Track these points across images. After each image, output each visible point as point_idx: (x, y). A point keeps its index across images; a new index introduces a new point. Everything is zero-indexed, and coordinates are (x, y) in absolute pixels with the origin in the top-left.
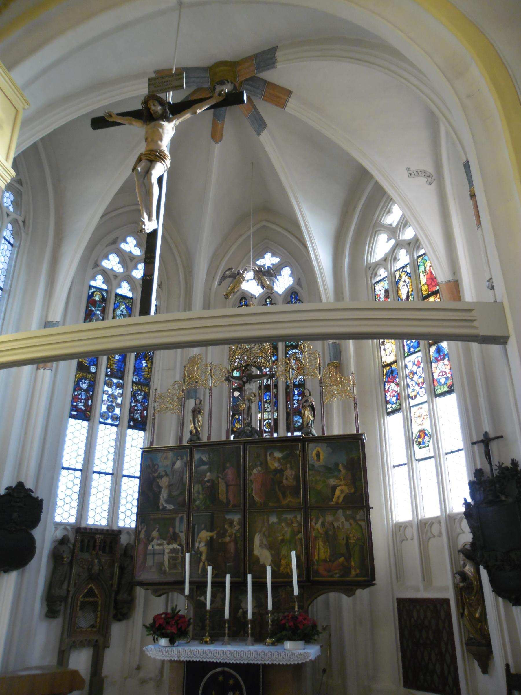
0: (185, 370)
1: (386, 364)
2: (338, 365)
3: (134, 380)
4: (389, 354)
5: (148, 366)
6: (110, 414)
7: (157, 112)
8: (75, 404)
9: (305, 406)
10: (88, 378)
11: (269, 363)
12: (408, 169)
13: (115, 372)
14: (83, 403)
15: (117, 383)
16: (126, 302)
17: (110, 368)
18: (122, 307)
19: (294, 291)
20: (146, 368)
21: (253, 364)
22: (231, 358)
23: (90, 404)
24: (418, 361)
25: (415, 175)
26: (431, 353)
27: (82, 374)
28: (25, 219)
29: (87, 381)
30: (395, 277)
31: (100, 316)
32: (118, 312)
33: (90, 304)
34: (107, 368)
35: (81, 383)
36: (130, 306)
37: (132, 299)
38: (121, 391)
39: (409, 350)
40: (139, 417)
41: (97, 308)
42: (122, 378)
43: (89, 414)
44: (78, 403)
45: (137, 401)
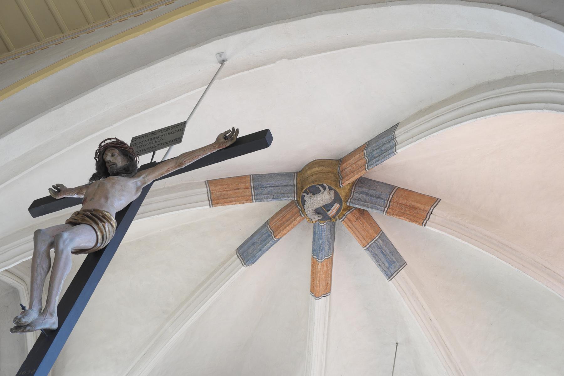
7: (115, 164)
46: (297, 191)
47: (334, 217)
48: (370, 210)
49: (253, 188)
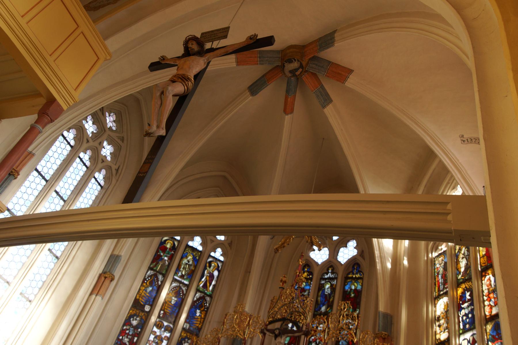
0: (225, 318)
1: (440, 342)
2: (386, 337)
3: (185, 326)
4: (443, 330)
5: (201, 316)
8: (121, 337)
10: (139, 316)
11: (306, 320)
12: (461, 136)
14: (129, 338)
15: (167, 326)
16: (194, 254)
17: (164, 310)
18: (190, 257)
19: (356, 262)
20: (200, 317)
21: (289, 318)
23: (135, 340)
24: (474, 339)
25: (468, 142)
26: (488, 331)
27: (136, 312)
28: (118, 168)
29: (138, 319)
30: (455, 249)
31: (167, 262)
32: (185, 261)
33: (161, 250)
34: (161, 310)
35: (132, 319)
36: (197, 258)
37: (200, 251)
38: (168, 335)
39: (464, 326)
41: (165, 254)
44: (124, 337)
46: (281, 61)
47: (299, 75)
48: (317, 73)
49: (259, 57)
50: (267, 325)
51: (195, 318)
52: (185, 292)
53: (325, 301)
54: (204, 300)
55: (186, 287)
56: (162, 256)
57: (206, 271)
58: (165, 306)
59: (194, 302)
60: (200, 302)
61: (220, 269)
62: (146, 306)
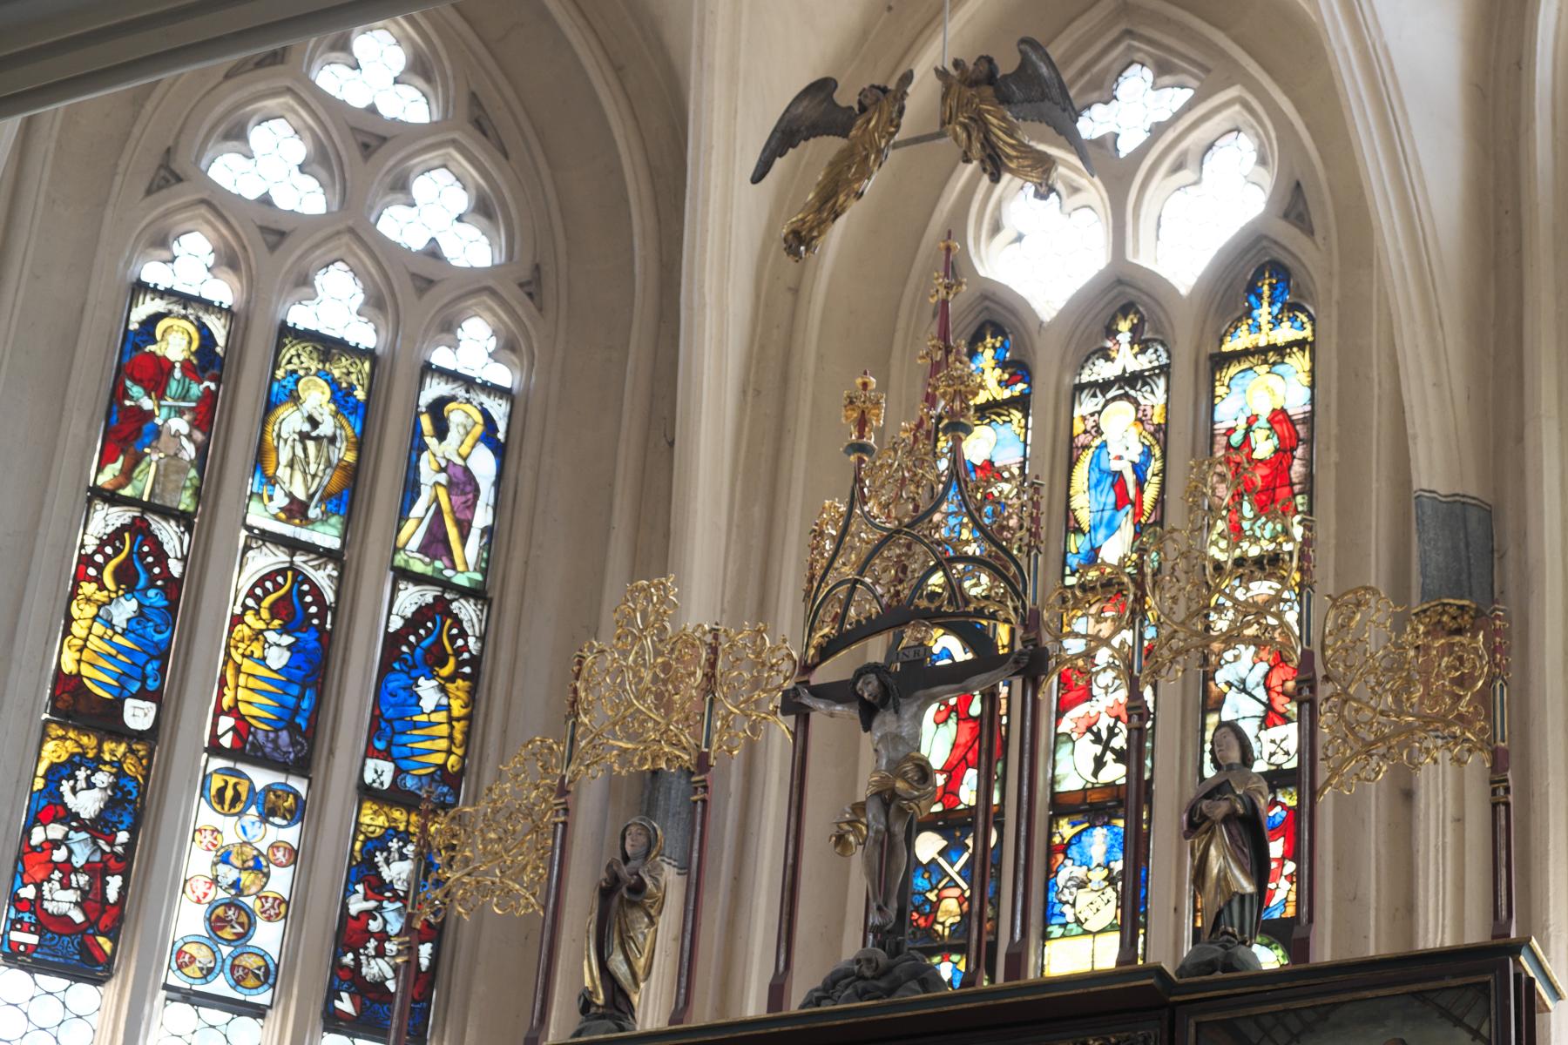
5: (449, 705)
6: (226, 950)
9: (1204, 818)
13: (261, 737)
15: (268, 789)
16: (337, 373)
18: (316, 397)
20: (441, 716)
22: (815, 584)
23: (112, 894)
34: (219, 712)
35: (66, 787)
36: (360, 394)
37: (369, 354)
38: (291, 835)
40: (389, 973)
42: (302, 767)
43: (107, 945)
44: (46, 887)
45: (378, 888)
50: (807, 669)
51: (416, 725)
52: (330, 597)
53: (1118, 506)
54: (449, 622)
55: (330, 567)
56: (150, 415)
57: (425, 456)
58: (237, 686)
59: (393, 640)
60: (429, 632)
61: (501, 436)
62: (130, 704)
